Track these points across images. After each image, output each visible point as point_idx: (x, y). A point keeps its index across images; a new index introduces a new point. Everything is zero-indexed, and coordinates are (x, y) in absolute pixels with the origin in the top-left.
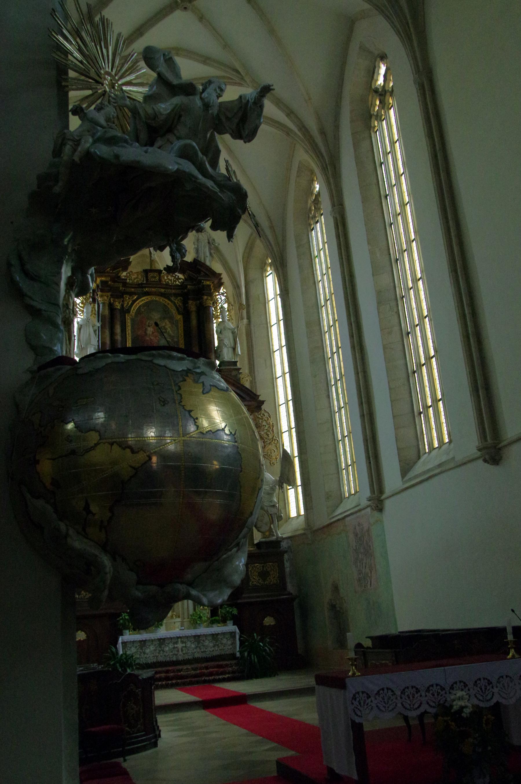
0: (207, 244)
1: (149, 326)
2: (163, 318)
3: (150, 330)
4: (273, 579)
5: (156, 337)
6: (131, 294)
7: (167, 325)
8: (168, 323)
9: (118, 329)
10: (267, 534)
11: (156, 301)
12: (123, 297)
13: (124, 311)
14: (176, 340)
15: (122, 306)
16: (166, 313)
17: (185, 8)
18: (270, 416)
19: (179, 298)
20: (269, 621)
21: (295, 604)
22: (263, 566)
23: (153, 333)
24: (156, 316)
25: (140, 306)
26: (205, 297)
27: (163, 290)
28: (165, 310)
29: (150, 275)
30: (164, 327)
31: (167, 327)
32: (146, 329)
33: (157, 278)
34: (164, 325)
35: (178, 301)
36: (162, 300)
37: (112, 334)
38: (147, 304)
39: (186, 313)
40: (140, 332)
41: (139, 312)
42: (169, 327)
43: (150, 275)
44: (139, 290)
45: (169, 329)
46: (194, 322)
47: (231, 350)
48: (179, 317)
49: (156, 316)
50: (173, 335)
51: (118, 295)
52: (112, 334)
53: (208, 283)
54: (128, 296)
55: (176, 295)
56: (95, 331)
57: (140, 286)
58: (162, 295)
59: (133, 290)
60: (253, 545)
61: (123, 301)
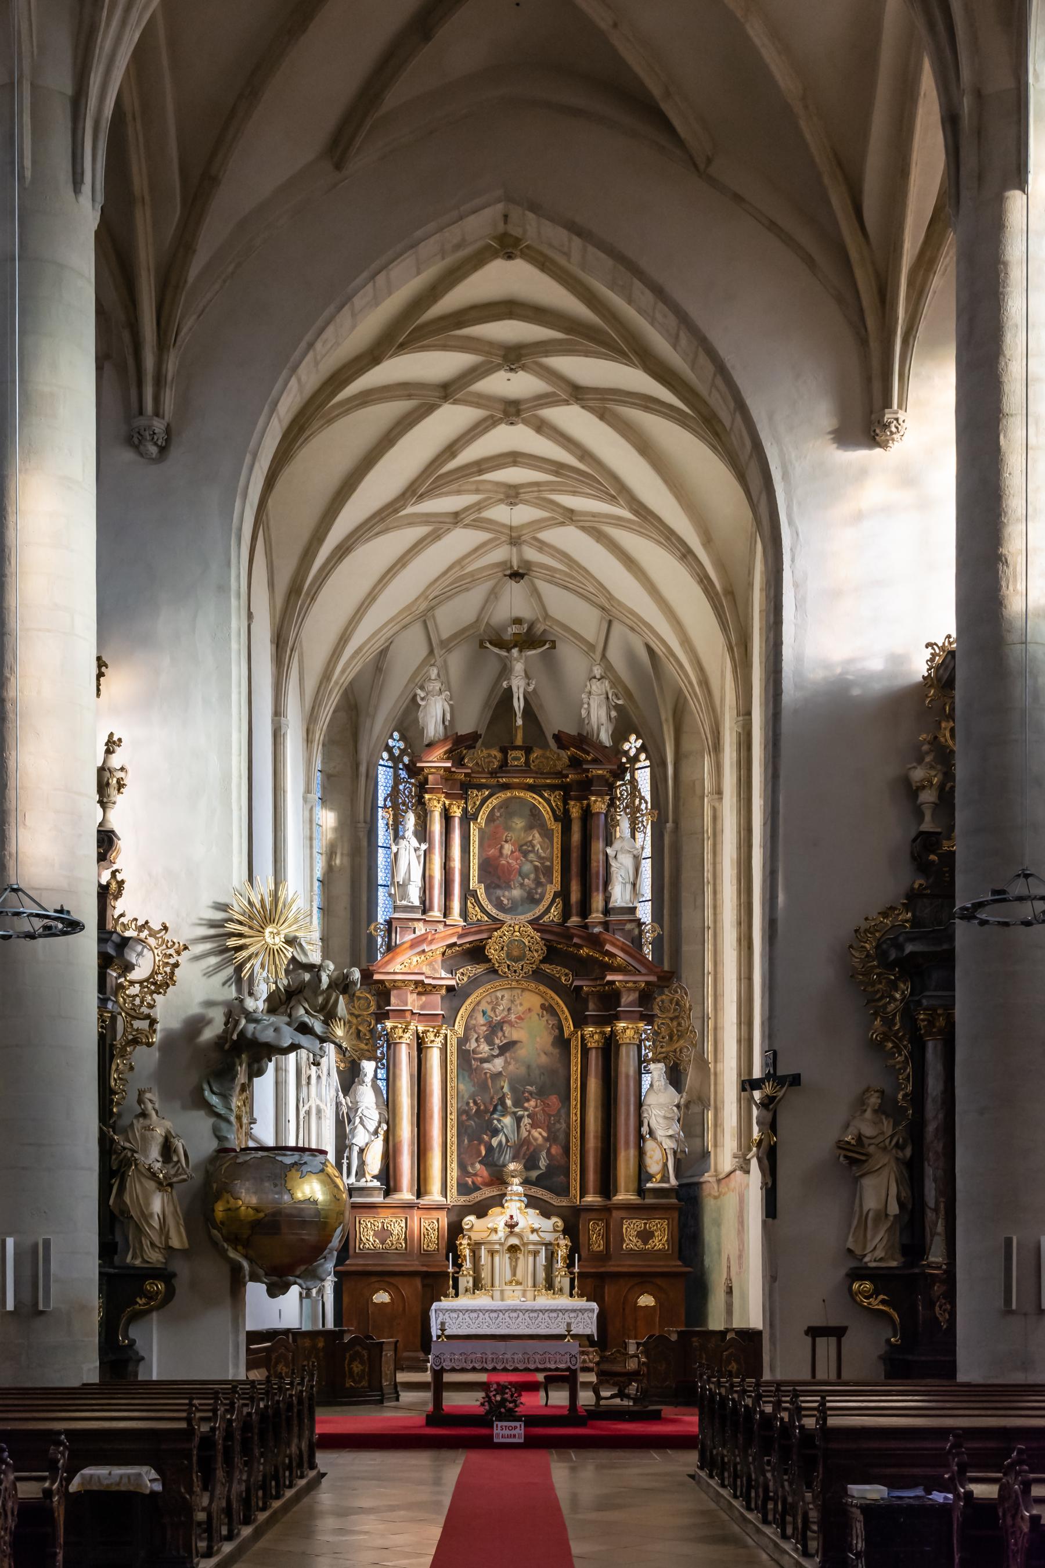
0: (605, 701)
1: (506, 841)
2: (530, 827)
3: (508, 848)
4: (660, 1241)
5: (517, 859)
6: (480, 787)
7: (536, 837)
8: (537, 835)
10: (658, 1177)
11: (519, 798)
12: (466, 793)
13: (467, 818)
14: (548, 863)
15: (465, 811)
17: (512, 424)
18: (686, 994)
19: (557, 793)
20: (646, 1300)
22: (645, 1224)
23: (512, 852)
25: (494, 808)
26: (593, 799)
27: (530, 781)
28: (534, 813)
29: (512, 754)
30: (531, 842)
31: (535, 842)
32: (502, 847)
33: (523, 760)
34: (530, 838)
36: (529, 796)
38: (505, 805)
39: (564, 819)
40: (492, 852)
41: (490, 819)
42: (539, 843)
43: (512, 754)
44: (493, 781)
45: (538, 846)
46: (576, 837)
47: (629, 887)
48: (556, 827)
49: (519, 823)
50: (543, 855)
53: (600, 772)
54: (475, 792)
55: (552, 788)
56: (418, 857)
57: (493, 774)
58: (531, 788)
59: (484, 781)
60: (641, 1192)
61: (466, 803)
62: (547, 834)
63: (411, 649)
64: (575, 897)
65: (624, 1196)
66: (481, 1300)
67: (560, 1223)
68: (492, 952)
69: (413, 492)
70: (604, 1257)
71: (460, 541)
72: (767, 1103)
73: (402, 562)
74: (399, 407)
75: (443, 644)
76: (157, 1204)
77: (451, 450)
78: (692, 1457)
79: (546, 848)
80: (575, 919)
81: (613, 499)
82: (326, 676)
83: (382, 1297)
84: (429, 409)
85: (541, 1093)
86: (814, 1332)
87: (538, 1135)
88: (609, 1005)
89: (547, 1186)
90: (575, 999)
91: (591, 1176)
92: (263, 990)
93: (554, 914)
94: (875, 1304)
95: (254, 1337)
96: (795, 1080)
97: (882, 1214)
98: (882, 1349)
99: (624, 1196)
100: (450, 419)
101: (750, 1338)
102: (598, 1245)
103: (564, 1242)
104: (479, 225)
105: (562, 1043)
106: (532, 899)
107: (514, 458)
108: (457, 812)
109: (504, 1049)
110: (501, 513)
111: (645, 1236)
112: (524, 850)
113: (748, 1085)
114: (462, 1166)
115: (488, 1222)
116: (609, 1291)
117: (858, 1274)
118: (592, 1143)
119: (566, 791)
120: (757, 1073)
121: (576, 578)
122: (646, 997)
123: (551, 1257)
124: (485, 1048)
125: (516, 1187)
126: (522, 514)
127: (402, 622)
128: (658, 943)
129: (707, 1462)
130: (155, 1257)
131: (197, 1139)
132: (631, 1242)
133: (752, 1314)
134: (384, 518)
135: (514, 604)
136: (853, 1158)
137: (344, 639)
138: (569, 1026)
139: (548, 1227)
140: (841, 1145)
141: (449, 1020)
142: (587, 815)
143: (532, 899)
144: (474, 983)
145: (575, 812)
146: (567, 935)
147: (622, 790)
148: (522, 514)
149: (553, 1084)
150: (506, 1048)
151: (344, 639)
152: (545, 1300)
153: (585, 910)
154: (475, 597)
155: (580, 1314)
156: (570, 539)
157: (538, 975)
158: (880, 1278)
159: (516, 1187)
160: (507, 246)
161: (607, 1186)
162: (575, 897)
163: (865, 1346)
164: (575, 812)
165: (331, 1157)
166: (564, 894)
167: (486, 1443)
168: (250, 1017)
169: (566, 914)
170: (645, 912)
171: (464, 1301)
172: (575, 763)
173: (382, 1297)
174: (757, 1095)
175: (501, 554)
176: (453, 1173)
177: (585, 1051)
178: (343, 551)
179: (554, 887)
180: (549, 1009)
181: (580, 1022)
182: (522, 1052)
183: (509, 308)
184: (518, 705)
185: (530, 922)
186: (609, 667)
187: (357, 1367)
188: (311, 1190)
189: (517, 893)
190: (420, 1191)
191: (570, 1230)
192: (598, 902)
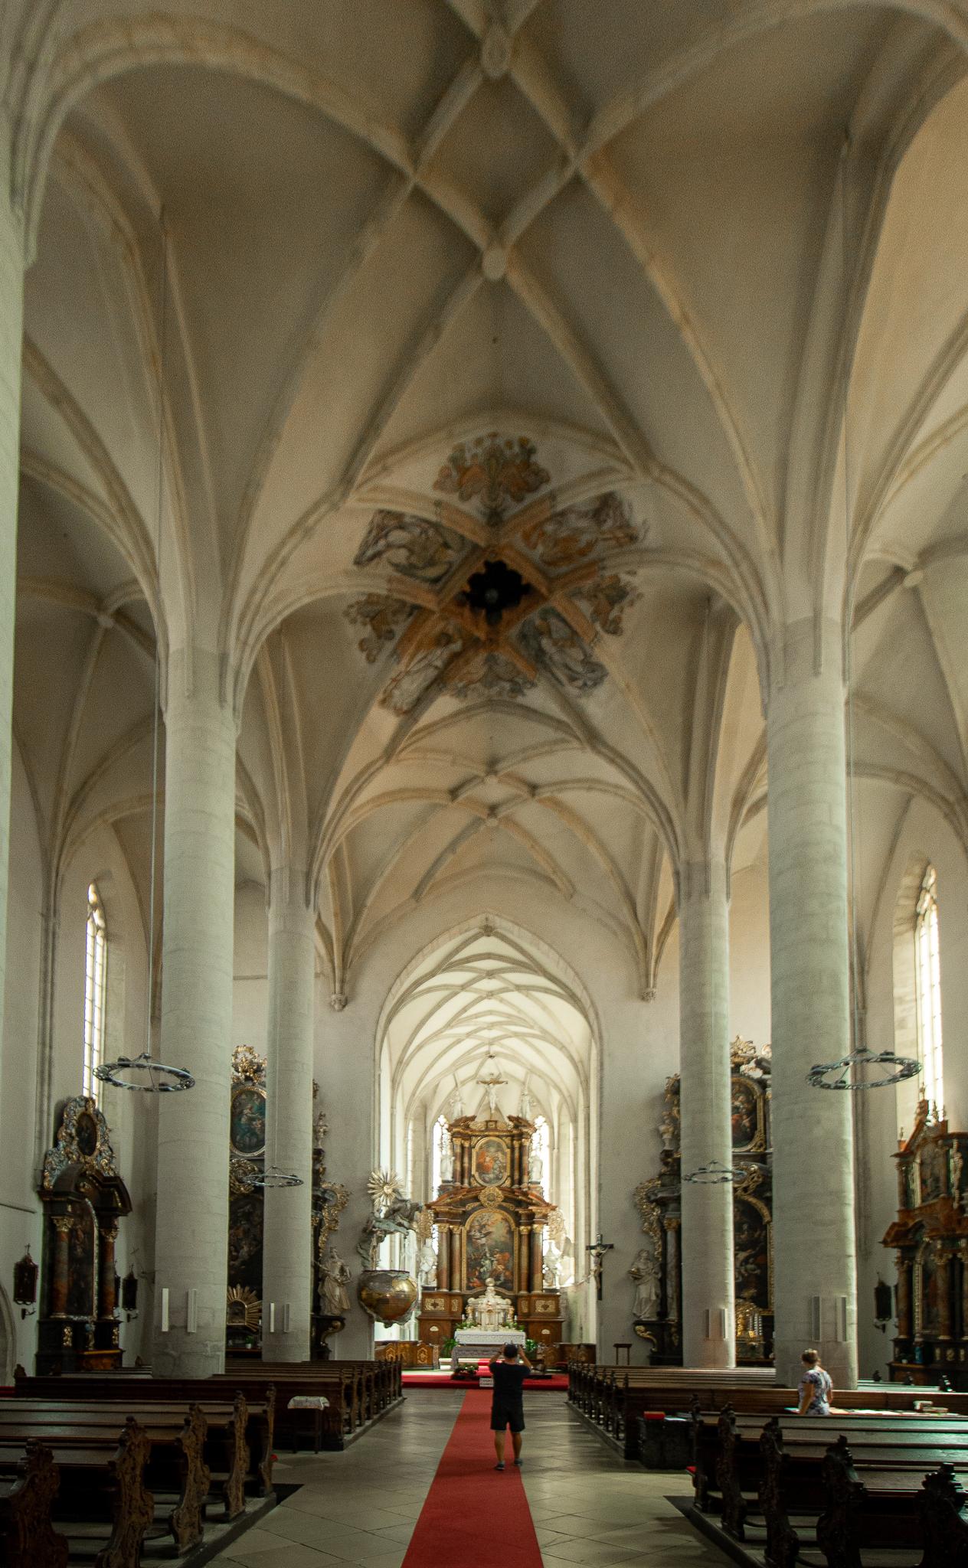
4: (551, 1309)
7: (500, 1155)
9: (466, 1160)
13: (471, 1147)
16: (499, 1148)
20: (546, 1332)
21: (564, 1325)
24: (492, 1150)
28: (499, 1146)
35: (508, 1140)
37: (462, 1163)
39: (512, 1149)
46: (517, 1154)
49: (492, 1150)
51: (468, 1137)
52: (462, 1163)
62: (504, 1154)
63: (447, 1085)
64: (516, 1176)
65: (537, 1292)
66: (475, 1331)
67: (509, 1301)
68: (481, 1198)
69: (449, 1025)
70: (528, 1315)
71: (468, 1044)
72: (599, 1255)
73: (445, 1052)
74: (445, 993)
75: (464, 1083)
76: (338, 1291)
77: (465, 1010)
78: (565, 1396)
79: (504, 1159)
80: (516, 1186)
81: (532, 1027)
82: (413, 1094)
83: (434, 1329)
84: (456, 994)
85: (501, 1252)
86: (617, 1346)
87: (500, 1268)
88: (531, 1218)
89: (504, 1287)
90: (517, 1217)
91: (524, 1284)
92: (384, 1210)
93: (508, 1183)
94: (646, 1335)
95: (379, 1344)
96: (611, 1247)
97: (649, 1300)
98: (648, 1353)
99: (537, 1292)
100: (464, 998)
101: (591, 1348)
102: (526, 1310)
103: (511, 1310)
104: (476, 923)
105: (511, 1232)
106: (498, 1178)
107: (491, 1013)
108: (467, 1145)
109: (487, 1234)
110: (486, 1034)
111: (546, 1307)
112: (495, 1160)
113: (589, 1248)
114: (468, 1279)
115: (479, 1301)
116: (531, 1327)
117: (638, 1323)
118: (524, 1271)
119: (512, 1137)
120: (593, 1243)
121: (514, 1058)
122: (545, 1216)
123: (506, 1315)
124: (478, 1235)
125: (491, 1288)
126: (495, 1033)
127: (444, 1074)
128: (551, 1195)
129: (572, 1397)
130: (336, 1312)
131: (355, 1269)
132: (539, 1309)
133: (592, 1338)
134: (437, 1034)
135: (490, 1068)
136: (636, 1277)
137: (421, 1081)
138: (513, 1226)
139: (505, 1303)
140: (630, 1272)
141: (463, 1224)
142: (521, 1147)
143: (498, 1178)
144: (474, 1210)
145: (516, 1144)
146: (513, 1192)
147: (535, 1136)
148: (495, 1033)
149: (506, 1248)
150: (488, 1234)
151: (421, 1081)
152: (503, 1331)
153: (520, 1182)
154: (475, 1064)
155: (517, 1337)
156: (514, 1043)
157: (500, 1207)
158: (647, 1325)
159: (491, 1288)
160: (488, 930)
161: (530, 1288)
162: (516, 1176)
163: (641, 1352)
164: (516, 1144)
165: (413, 1274)
166: (512, 1176)
167: (477, 1387)
168: (378, 1220)
169: (513, 1183)
170: (545, 1184)
171: (467, 1331)
172: (516, 1127)
173: (434, 1329)
174: (593, 1252)
175: (485, 1049)
176: (465, 1282)
177: (520, 1236)
178: (420, 1047)
179: (508, 1173)
180: (506, 1220)
181: (518, 1224)
182: (493, 1236)
183: (488, 956)
184: (493, 1106)
185: (499, 1187)
186: (530, 1091)
187: (423, 1355)
188: (404, 1287)
189: (491, 1176)
190: (451, 1288)
191: (514, 1304)
192: (525, 1178)
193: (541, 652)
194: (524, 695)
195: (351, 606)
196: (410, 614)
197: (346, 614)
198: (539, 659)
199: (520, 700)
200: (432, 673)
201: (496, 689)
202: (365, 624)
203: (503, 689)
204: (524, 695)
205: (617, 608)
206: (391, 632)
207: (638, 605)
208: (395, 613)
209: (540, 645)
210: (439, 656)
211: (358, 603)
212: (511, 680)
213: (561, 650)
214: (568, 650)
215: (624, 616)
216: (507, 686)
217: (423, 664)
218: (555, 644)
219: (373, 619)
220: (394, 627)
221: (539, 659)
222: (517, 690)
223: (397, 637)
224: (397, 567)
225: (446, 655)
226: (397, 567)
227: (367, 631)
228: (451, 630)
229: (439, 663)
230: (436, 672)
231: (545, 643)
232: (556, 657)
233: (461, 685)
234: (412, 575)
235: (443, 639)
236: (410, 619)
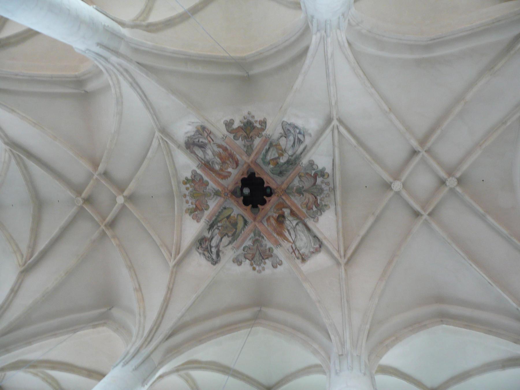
193: (288, 162)
194: (324, 169)
195: (254, 269)
196: (263, 237)
197: (259, 272)
198: (293, 162)
199: (329, 170)
200: (300, 227)
201: (323, 186)
202: (265, 263)
203: (322, 182)
204: (324, 169)
205: (255, 125)
206: (269, 249)
207: (253, 113)
208: (261, 246)
209: (285, 163)
210: (290, 222)
211: (251, 265)
212: (315, 177)
213: (285, 151)
214: (283, 147)
215: (258, 120)
216: (319, 180)
217: (292, 232)
218: (282, 155)
219: (263, 258)
220: (267, 247)
221: (293, 162)
222: (322, 173)
223: (272, 246)
224: (230, 243)
225: (290, 218)
226: (230, 243)
227: (269, 262)
228: (276, 215)
229: (294, 223)
230: (300, 225)
231: (283, 160)
232: (290, 153)
233: (315, 209)
234: (239, 236)
235: (281, 219)
236: (265, 238)
